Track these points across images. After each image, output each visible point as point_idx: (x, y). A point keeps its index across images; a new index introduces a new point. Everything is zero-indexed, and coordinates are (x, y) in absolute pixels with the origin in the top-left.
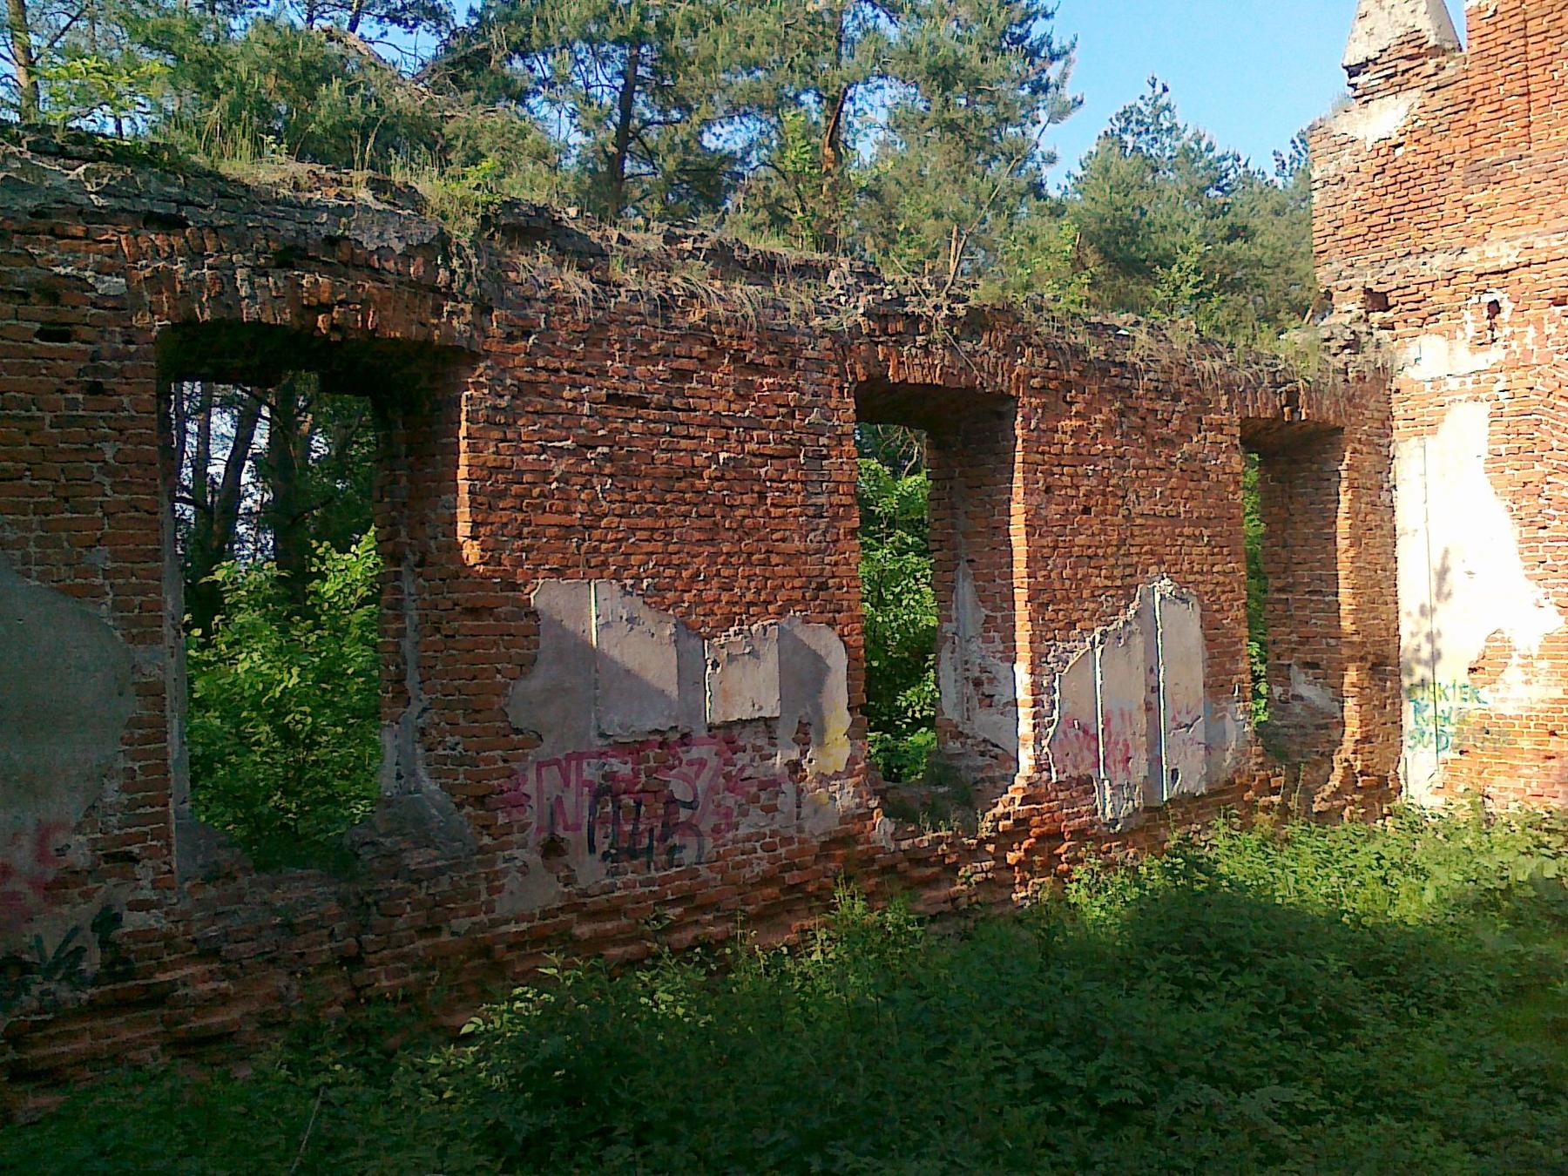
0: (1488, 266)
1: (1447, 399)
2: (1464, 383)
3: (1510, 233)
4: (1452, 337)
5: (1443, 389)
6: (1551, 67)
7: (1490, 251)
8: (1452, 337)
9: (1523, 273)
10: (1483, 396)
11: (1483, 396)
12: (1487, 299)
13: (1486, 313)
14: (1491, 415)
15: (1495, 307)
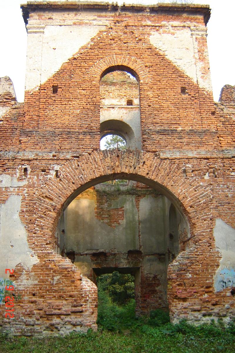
0: (25, 158)
1: (9, 194)
2: (14, 190)
3: (32, 150)
4: (12, 176)
5: (9, 190)
6: (45, 111)
7: (26, 154)
8: (12, 176)
9: (35, 162)
10: (20, 194)
11: (20, 194)
12: (24, 167)
13: (23, 171)
14: (22, 200)
15: (26, 170)
